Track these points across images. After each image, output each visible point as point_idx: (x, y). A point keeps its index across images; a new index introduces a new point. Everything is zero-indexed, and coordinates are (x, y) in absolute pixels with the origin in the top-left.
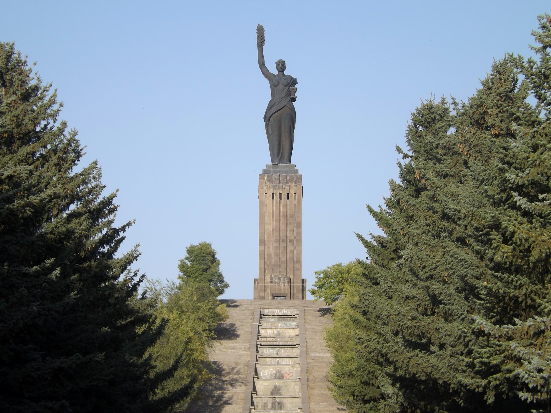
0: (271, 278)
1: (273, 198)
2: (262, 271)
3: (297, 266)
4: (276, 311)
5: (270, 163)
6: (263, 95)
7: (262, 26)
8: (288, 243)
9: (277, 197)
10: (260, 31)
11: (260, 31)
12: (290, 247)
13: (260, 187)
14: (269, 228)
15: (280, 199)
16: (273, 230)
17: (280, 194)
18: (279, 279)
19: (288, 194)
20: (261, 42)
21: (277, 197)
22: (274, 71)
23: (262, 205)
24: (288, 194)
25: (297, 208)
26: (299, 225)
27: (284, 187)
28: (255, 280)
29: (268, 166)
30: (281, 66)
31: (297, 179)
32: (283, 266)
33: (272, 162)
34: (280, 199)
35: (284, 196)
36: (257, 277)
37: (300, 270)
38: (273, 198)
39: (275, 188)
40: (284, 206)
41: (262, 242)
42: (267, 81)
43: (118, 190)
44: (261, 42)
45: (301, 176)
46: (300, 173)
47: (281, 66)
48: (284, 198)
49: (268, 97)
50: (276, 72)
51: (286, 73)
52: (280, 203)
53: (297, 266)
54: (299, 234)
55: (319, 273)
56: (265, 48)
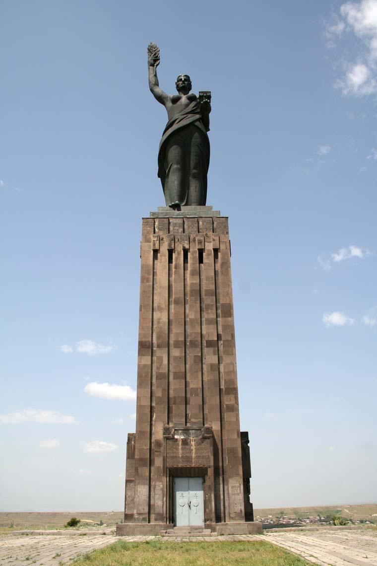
0: (166, 431)
2: (146, 414)
3: (227, 401)
6: (155, 123)
8: (205, 350)
9: (178, 257)
12: (210, 358)
14: (161, 317)
17: (186, 252)
18: (186, 431)
21: (178, 257)
23: (148, 276)
25: (222, 273)
26: (228, 311)
28: (130, 438)
30: (184, 85)
31: (220, 225)
32: (195, 401)
35: (192, 257)
36: (133, 431)
37: (234, 409)
40: (193, 274)
47: (184, 85)
48: (194, 258)
52: (185, 269)
53: (227, 401)
54: (230, 328)
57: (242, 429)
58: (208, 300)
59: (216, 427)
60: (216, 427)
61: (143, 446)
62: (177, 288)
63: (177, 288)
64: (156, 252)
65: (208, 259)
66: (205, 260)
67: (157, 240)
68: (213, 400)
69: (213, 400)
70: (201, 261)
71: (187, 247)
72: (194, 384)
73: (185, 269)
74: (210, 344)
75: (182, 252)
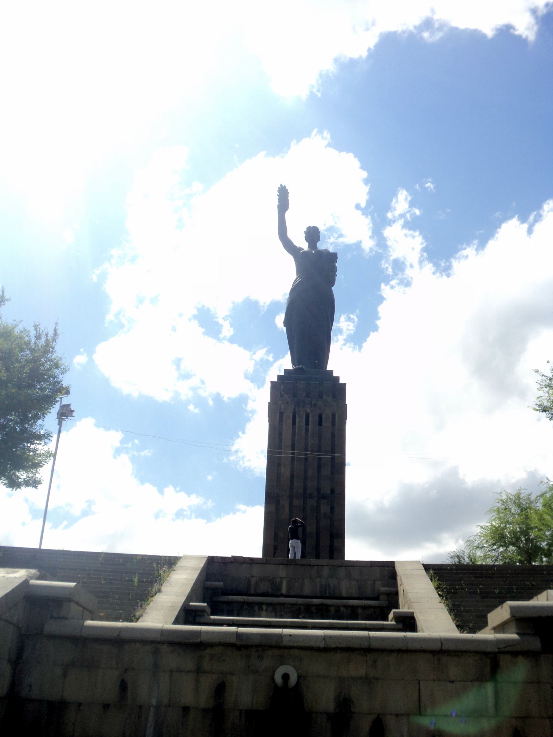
1: (294, 423)
7: (285, 187)
10: (283, 194)
11: (283, 194)
15: (307, 423)
16: (292, 477)
19: (320, 417)
24: (320, 417)
27: (313, 403)
29: (286, 371)
30: (313, 235)
34: (307, 423)
38: (294, 423)
45: (345, 384)
50: (305, 246)
51: (321, 246)
52: (307, 430)
56: (288, 214)
64: (281, 414)
65: (326, 423)
66: (324, 424)
67: (283, 404)
69: (325, 542)
70: (320, 424)
71: (308, 411)
73: (307, 430)
74: (324, 497)
75: (304, 417)
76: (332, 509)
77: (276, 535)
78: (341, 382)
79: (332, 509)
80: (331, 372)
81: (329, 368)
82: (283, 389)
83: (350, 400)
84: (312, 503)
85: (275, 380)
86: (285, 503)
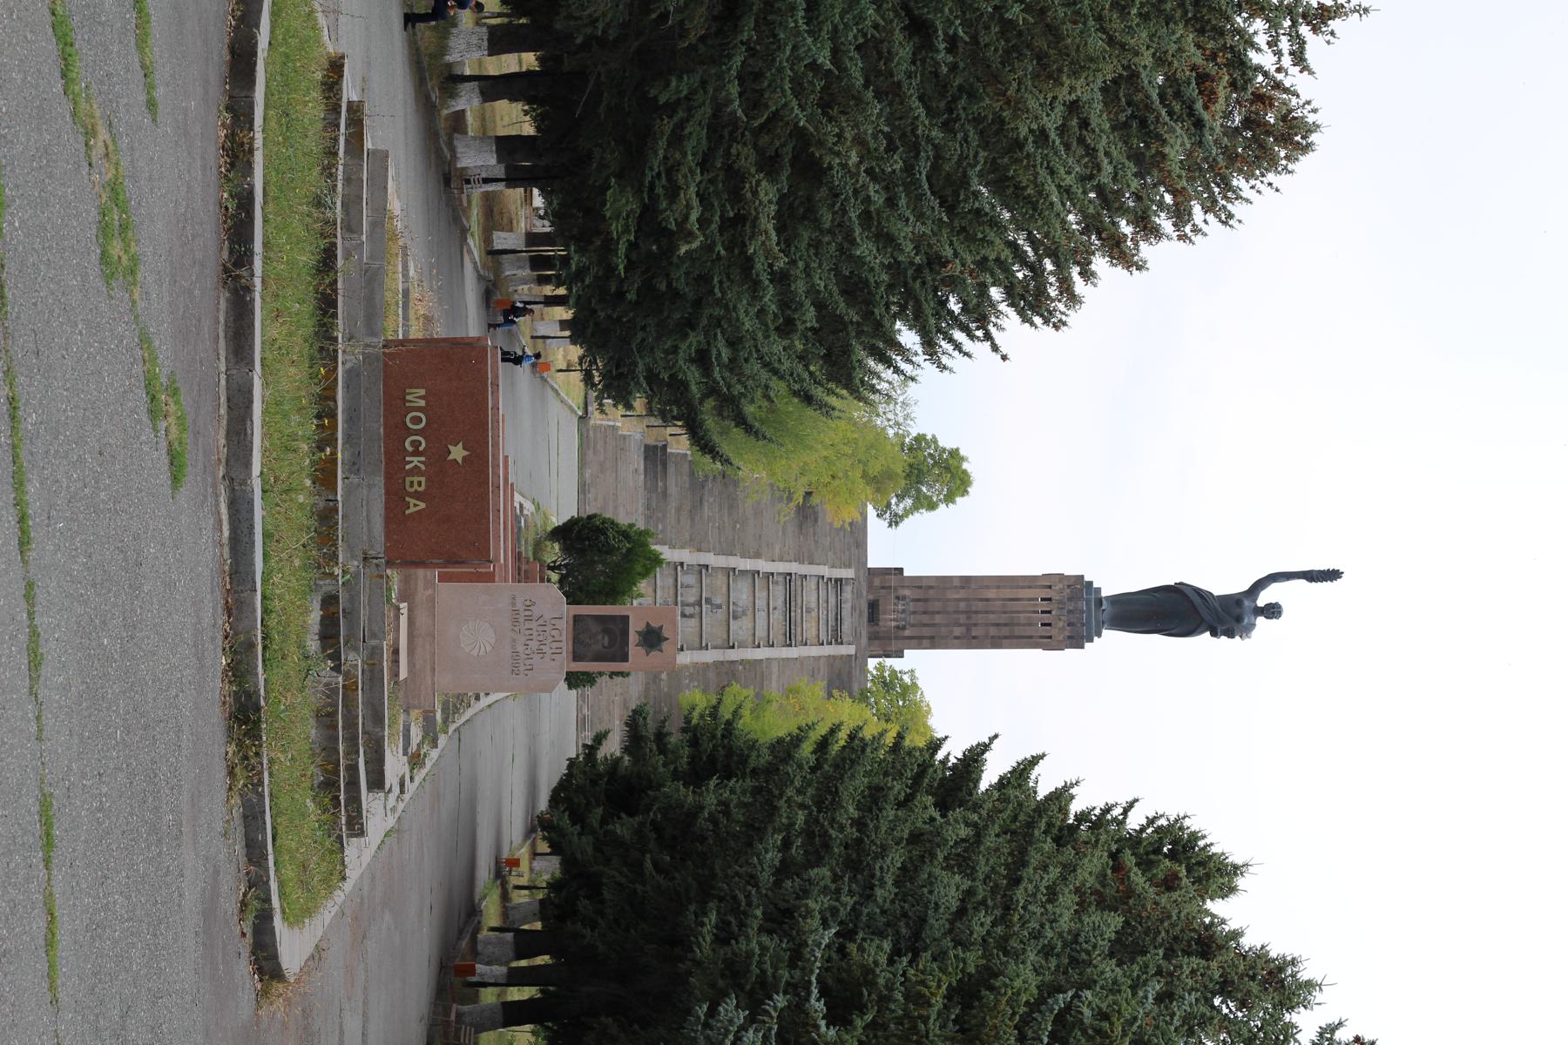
0: (904, 598)
2: (919, 583)
4: (847, 607)
5: (1104, 594)
9: (1045, 606)
10: (1332, 575)
11: (1332, 575)
12: (958, 631)
13: (1061, 576)
14: (991, 594)
20: (1312, 576)
21: (1045, 606)
22: (1263, 599)
28: (901, 570)
29: (1099, 590)
30: (1273, 611)
32: (925, 619)
33: (1107, 598)
39: (1060, 602)
41: (966, 581)
42: (1246, 587)
43: (1004, 358)
44: (1312, 576)
46: (1087, 645)
47: (1273, 611)
49: (1218, 590)
50: (1261, 602)
51: (1261, 620)
55: (913, 677)
57: (906, 652)
58: (1005, 631)
59: (907, 633)
60: (907, 633)
61: (893, 581)
62: (1018, 606)
63: (1018, 606)
68: (926, 632)
69: (926, 632)
72: (938, 619)
74: (968, 630)
76: (957, 638)
77: (931, 587)
78: (1087, 645)
79: (957, 638)
80: (1099, 635)
81: (1105, 632)
82: (1079, 587)
83: (1070, 653)
84: (962, 618)
85: (1087, 579)
86: (962, 594)
